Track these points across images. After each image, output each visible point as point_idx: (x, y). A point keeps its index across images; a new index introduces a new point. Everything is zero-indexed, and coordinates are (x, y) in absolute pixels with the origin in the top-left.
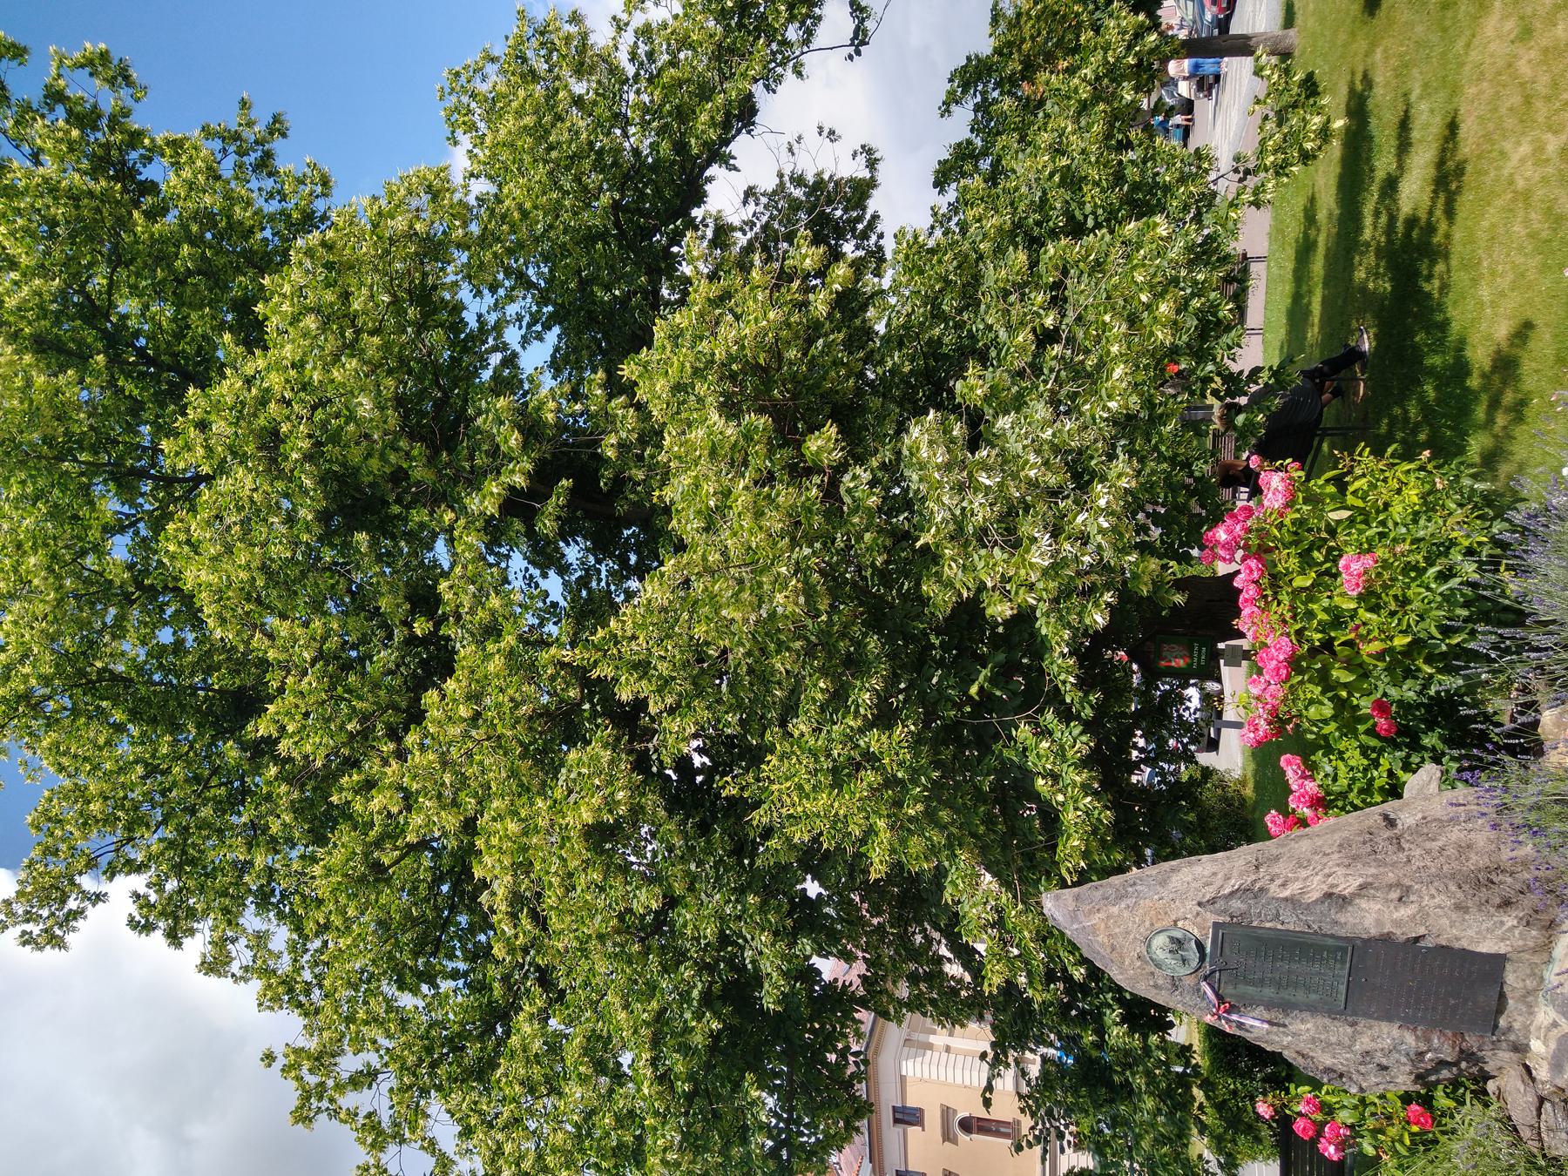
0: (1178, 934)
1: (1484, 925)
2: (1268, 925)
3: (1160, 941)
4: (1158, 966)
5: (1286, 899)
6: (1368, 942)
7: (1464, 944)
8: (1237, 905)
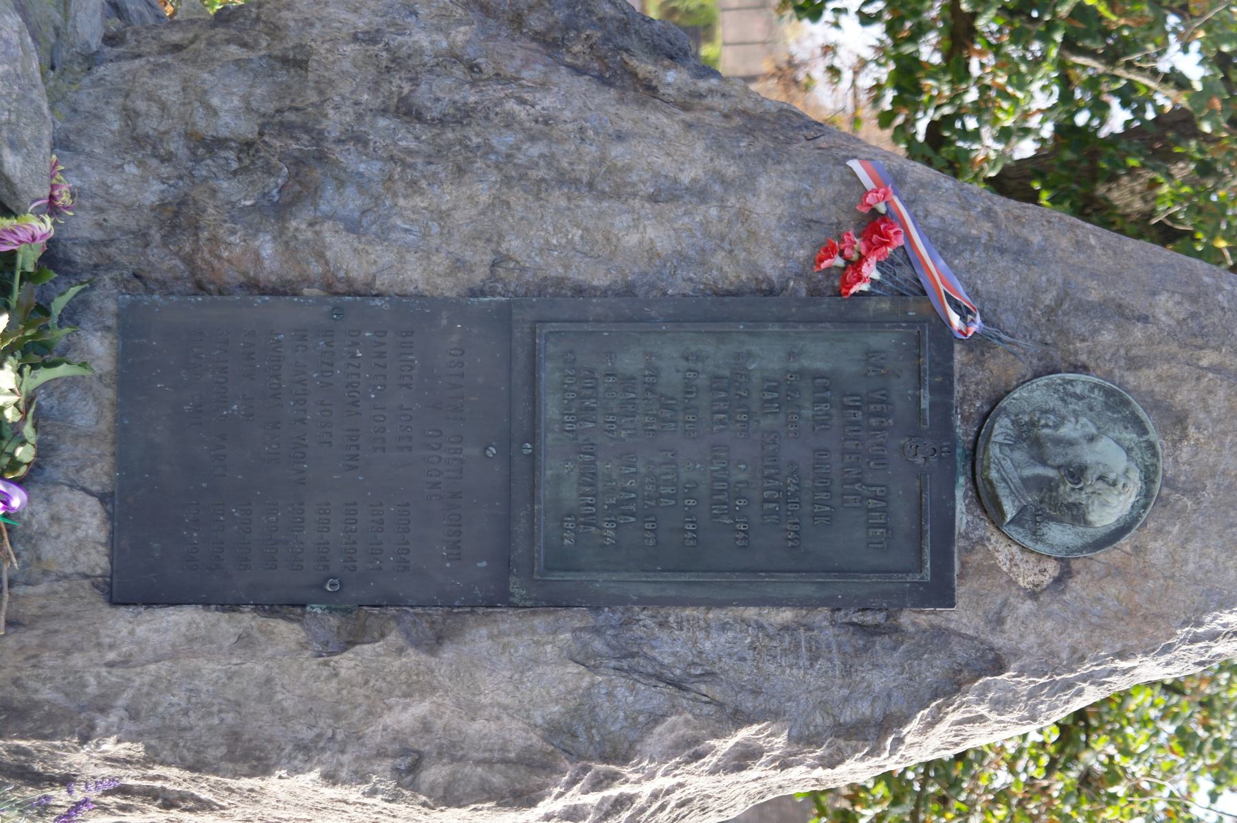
0: (1059, 535)
1: (179, 698)
2: (786, 615)
3: (1108, 511)
4: (1116, 401)
5: (740, 718)
6: (496, 599)
7: (225, 626)
8: (882, 677)
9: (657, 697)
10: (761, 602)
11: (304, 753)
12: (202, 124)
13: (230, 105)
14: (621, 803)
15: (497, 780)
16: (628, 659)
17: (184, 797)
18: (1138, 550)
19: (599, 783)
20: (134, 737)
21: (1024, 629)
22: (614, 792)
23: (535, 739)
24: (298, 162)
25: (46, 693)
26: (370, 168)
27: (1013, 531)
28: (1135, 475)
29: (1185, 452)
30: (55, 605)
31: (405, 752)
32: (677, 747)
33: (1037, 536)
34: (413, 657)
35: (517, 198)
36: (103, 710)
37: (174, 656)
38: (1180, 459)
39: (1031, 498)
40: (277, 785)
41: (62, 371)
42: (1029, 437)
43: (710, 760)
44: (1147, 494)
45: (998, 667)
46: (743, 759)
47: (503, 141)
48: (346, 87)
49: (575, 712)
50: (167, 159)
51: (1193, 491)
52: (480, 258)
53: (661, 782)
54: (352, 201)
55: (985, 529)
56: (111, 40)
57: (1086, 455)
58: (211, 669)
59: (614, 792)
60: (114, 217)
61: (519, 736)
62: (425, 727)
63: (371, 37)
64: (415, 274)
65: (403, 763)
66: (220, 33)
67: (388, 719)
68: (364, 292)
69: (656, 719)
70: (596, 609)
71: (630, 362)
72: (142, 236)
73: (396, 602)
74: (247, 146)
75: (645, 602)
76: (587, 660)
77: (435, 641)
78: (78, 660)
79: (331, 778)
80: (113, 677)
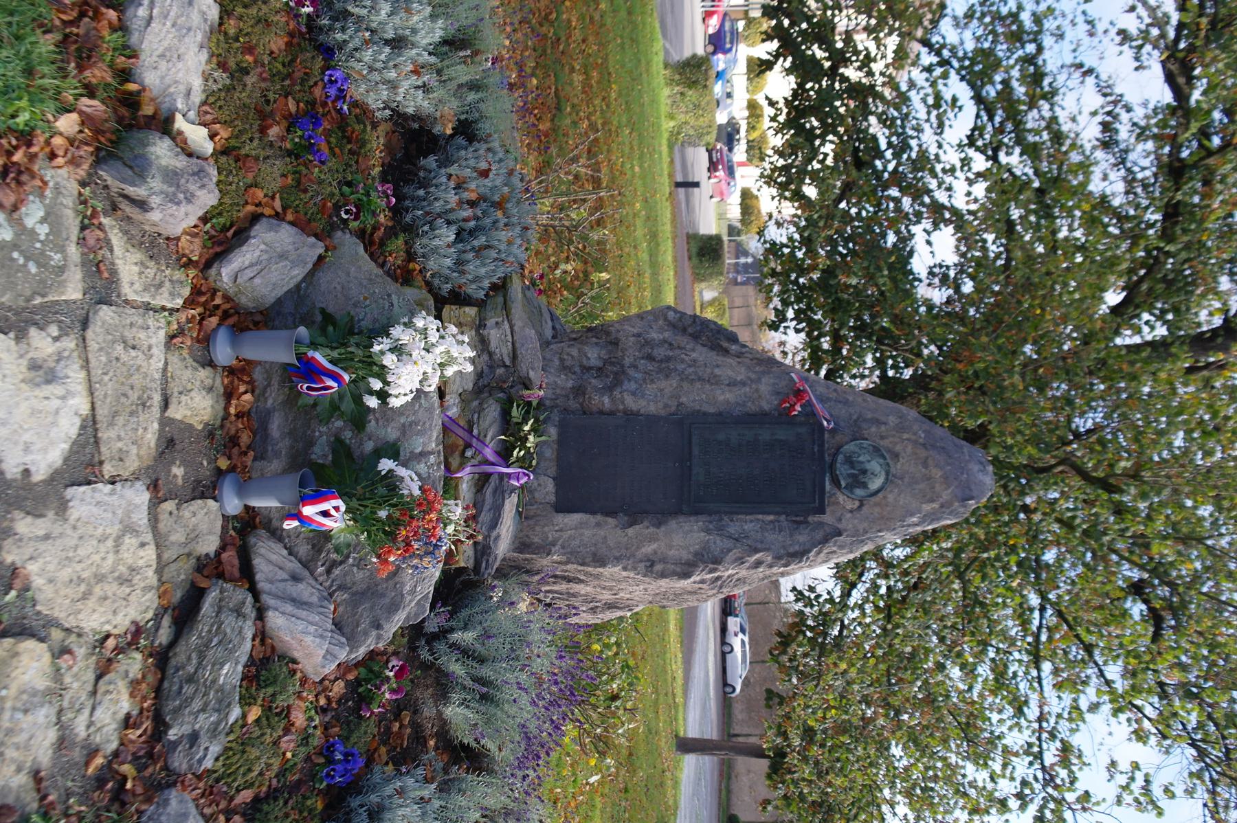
0: (859, 492)
1: (577, 542)
2: (771, 517)
3: (875, 484)
4: (877, 451)
5: (756, 551)
6: (677, 512)
7: (592, 519)
8: (802, 538)
9: (728, 543)
10: (763, 513)
11: (618, 559)
12: (585, 362)
13: (594, 355)
14: (718, 578)
15: (678, 570)
16: (720, 529)
17: (574, 578)
18: (885, 497)
19: (710, 572)
20: (564, 554)
21: (848, 523)
22: (716, 575)
23: (690, 557)
24: (616, 374)
25: (536, 540)
26: (639, 376)
27: (846, 492)
28: (883, 473)
29: (899, 466)
30: (539, 512)
31: (649, 560)
32: (736, 560)
33: (852, 493)
34: (652, 529)
35: (685, 385)
36: (554, 546)
37: (576, 528)
38: (897, 468)
39: (850, 480)
40: (607, 571)
41: (543, 438)
42: (850, 461)
43: (747, 565)
44: (887, 479)
45: (840, 534)
46: (758, 564)
47: (681, 367)
48: (631, 351)
49: (704, 548)
50: (574, 373)
51: (902, 478)
52: (673, 403)
53: (730, 572)
54: (633, 386)
55: (836, 490)
56: (554, 337)
57: (868, 466)
58: (588, 532)
59: (716, 575)
60: (558, 391)
61: (685, 556)
62: (656, 553)
63: (639, 335)
64: (652, 409)
65: (648, 564)
66: (590, 334)
67: (643, 550)
68: (637, 414)
69: (730, 550)
70: (710, 515)
71: (721, 436)
72: (567, 396)
73: (646, 512)
74: (599, 369)
75: (726, 513)
76: (708, 531)
77: (658, 525)
78: (546, 529)
79: (625, 569)
80: (557, 535)
